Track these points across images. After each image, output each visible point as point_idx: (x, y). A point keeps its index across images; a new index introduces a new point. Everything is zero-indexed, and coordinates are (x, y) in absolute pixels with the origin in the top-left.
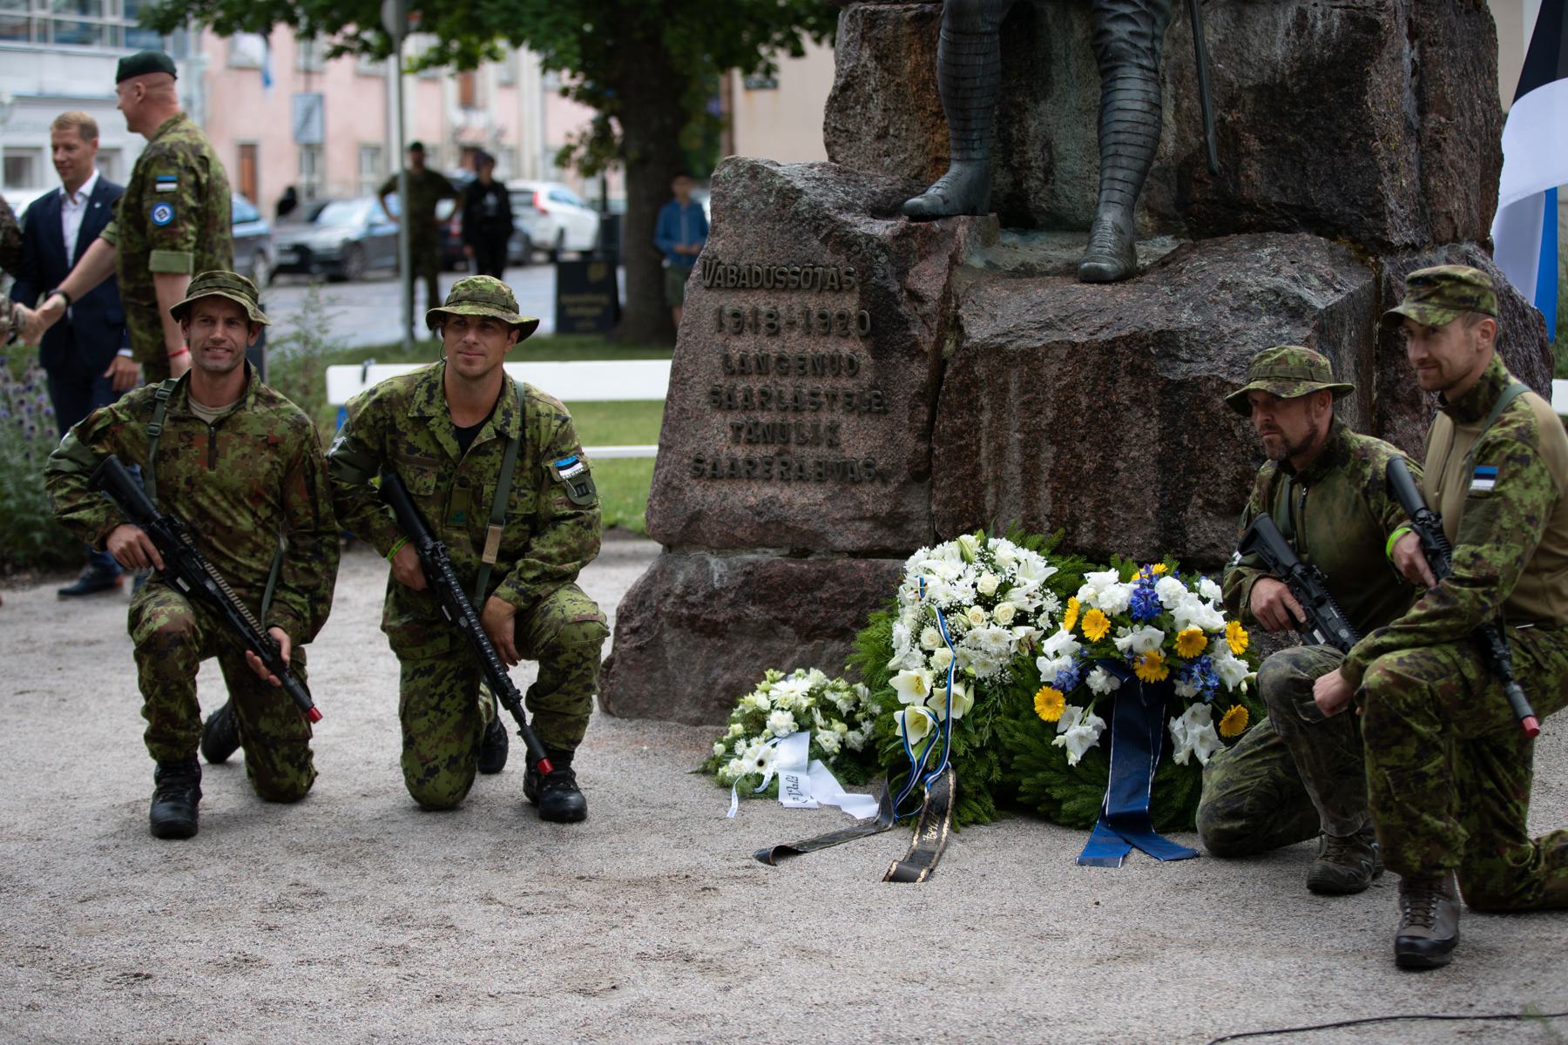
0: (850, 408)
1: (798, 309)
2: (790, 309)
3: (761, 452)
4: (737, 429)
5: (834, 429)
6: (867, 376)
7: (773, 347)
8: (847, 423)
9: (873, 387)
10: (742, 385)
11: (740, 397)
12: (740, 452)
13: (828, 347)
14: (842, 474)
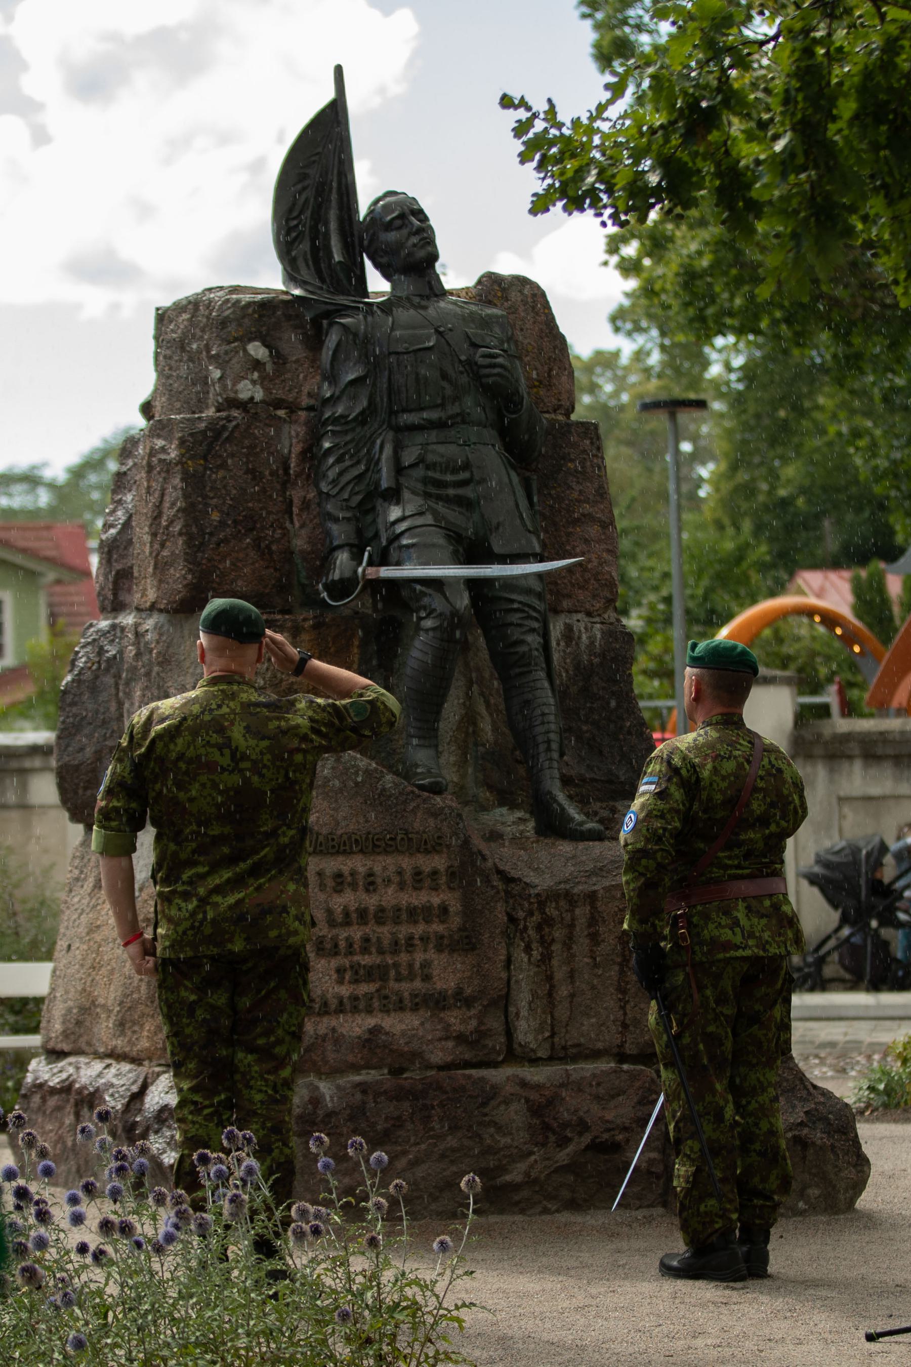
0: (440, 949)
1: (392, 868)
2: (385, 868)
3: (364, 988)
4: (340, 971)
5: (426, 965)
6: (456, 921)
7: (372, 902)
8: (439, 961)
9: (460, 930)
10: (343, 934)
11: (342, 944)
12: (345, 991)
13: (420, 898)
14: (436, 1003)
